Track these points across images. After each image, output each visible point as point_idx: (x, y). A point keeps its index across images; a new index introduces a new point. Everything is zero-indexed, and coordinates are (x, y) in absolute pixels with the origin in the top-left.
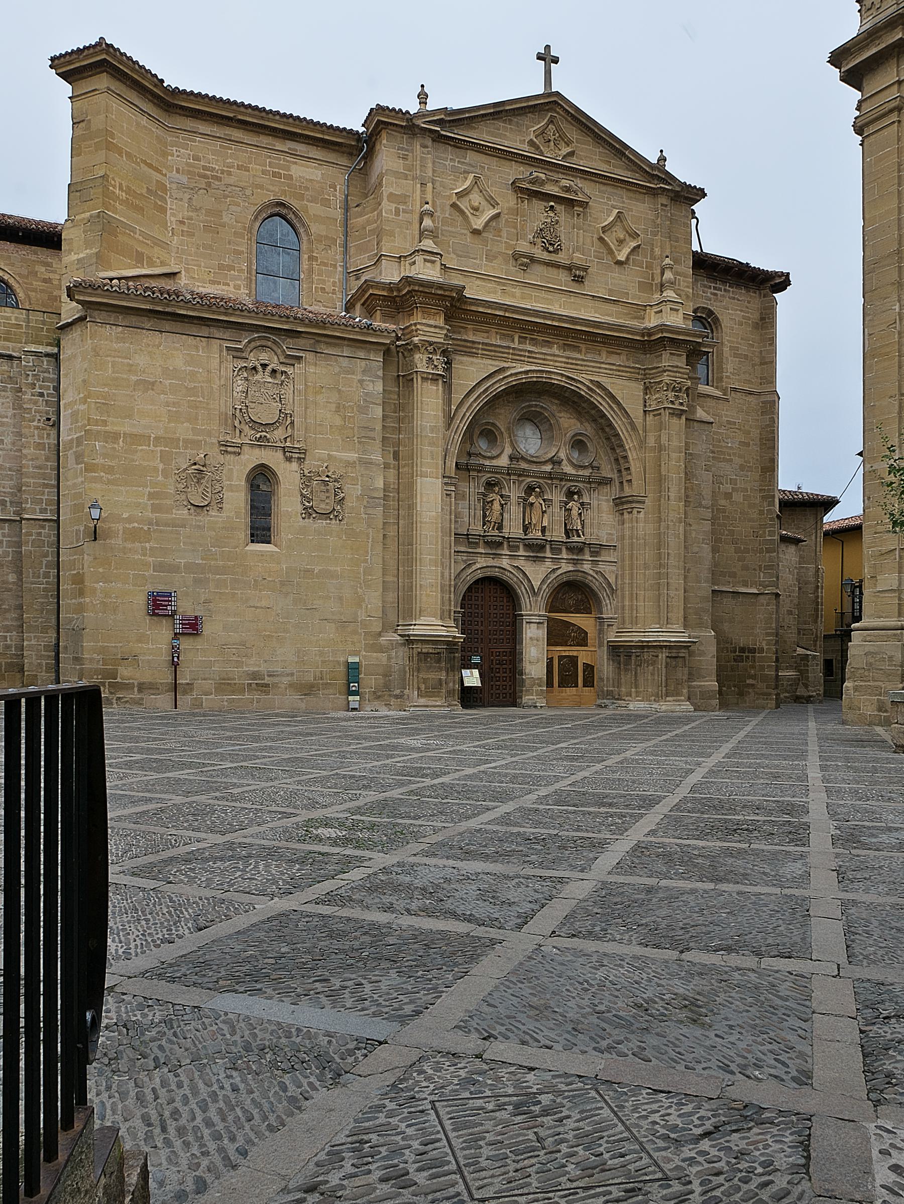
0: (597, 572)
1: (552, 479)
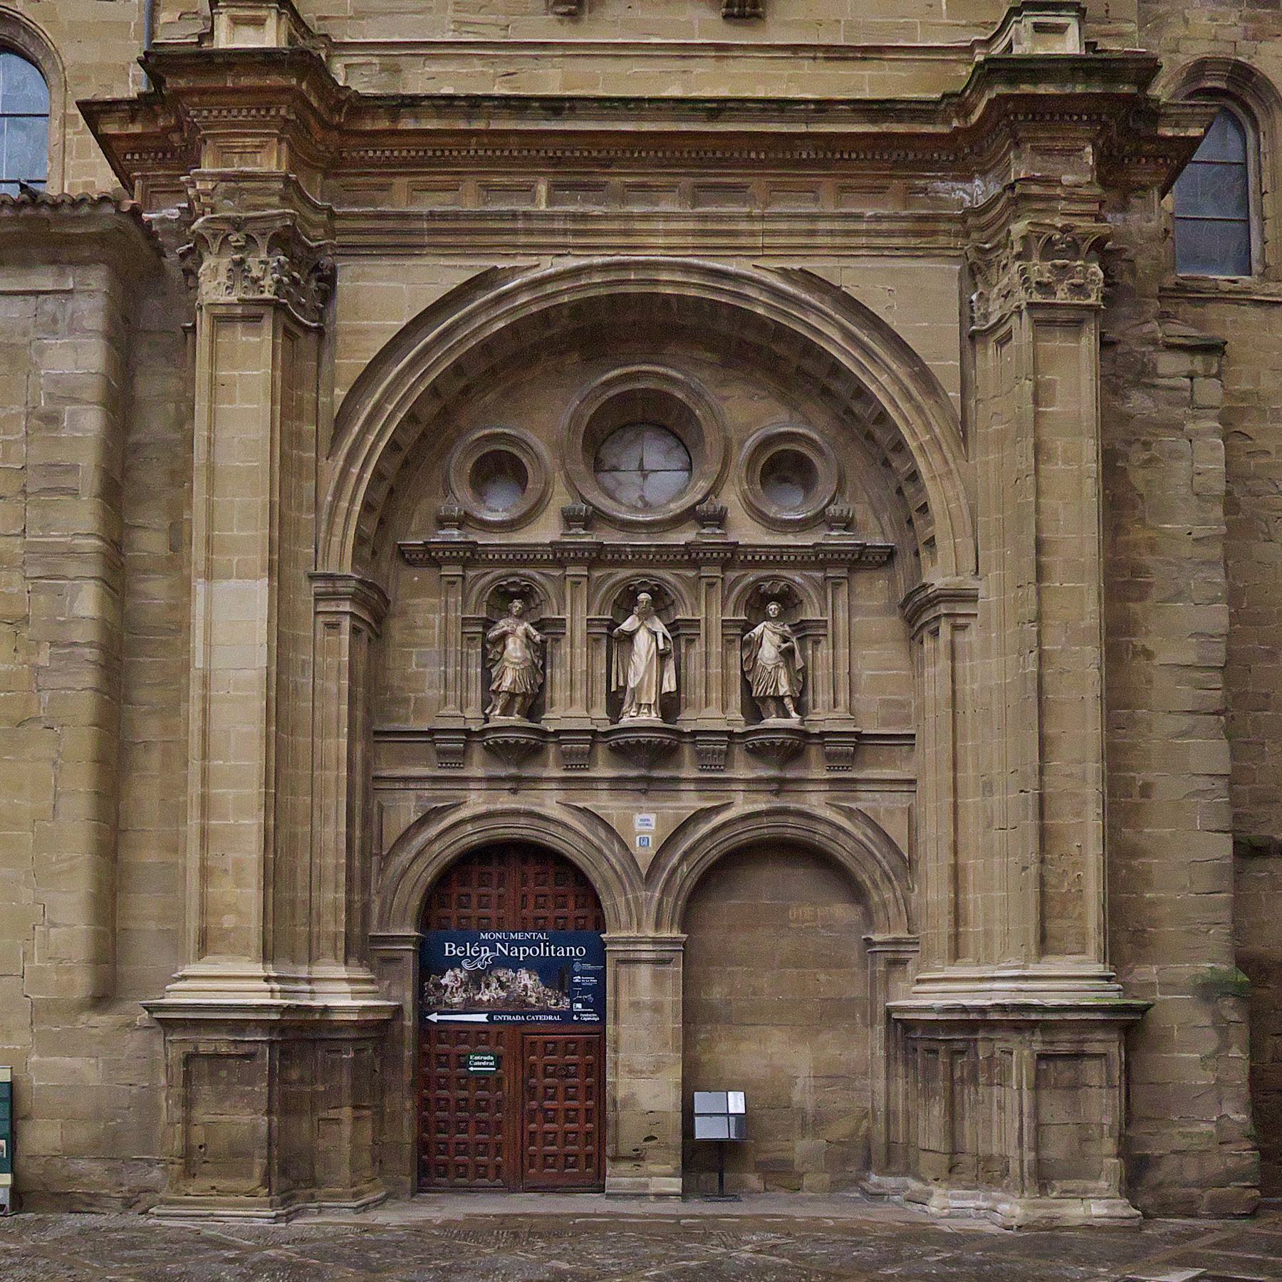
0: (850, 813)
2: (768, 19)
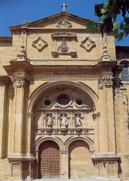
0: (87, 137)
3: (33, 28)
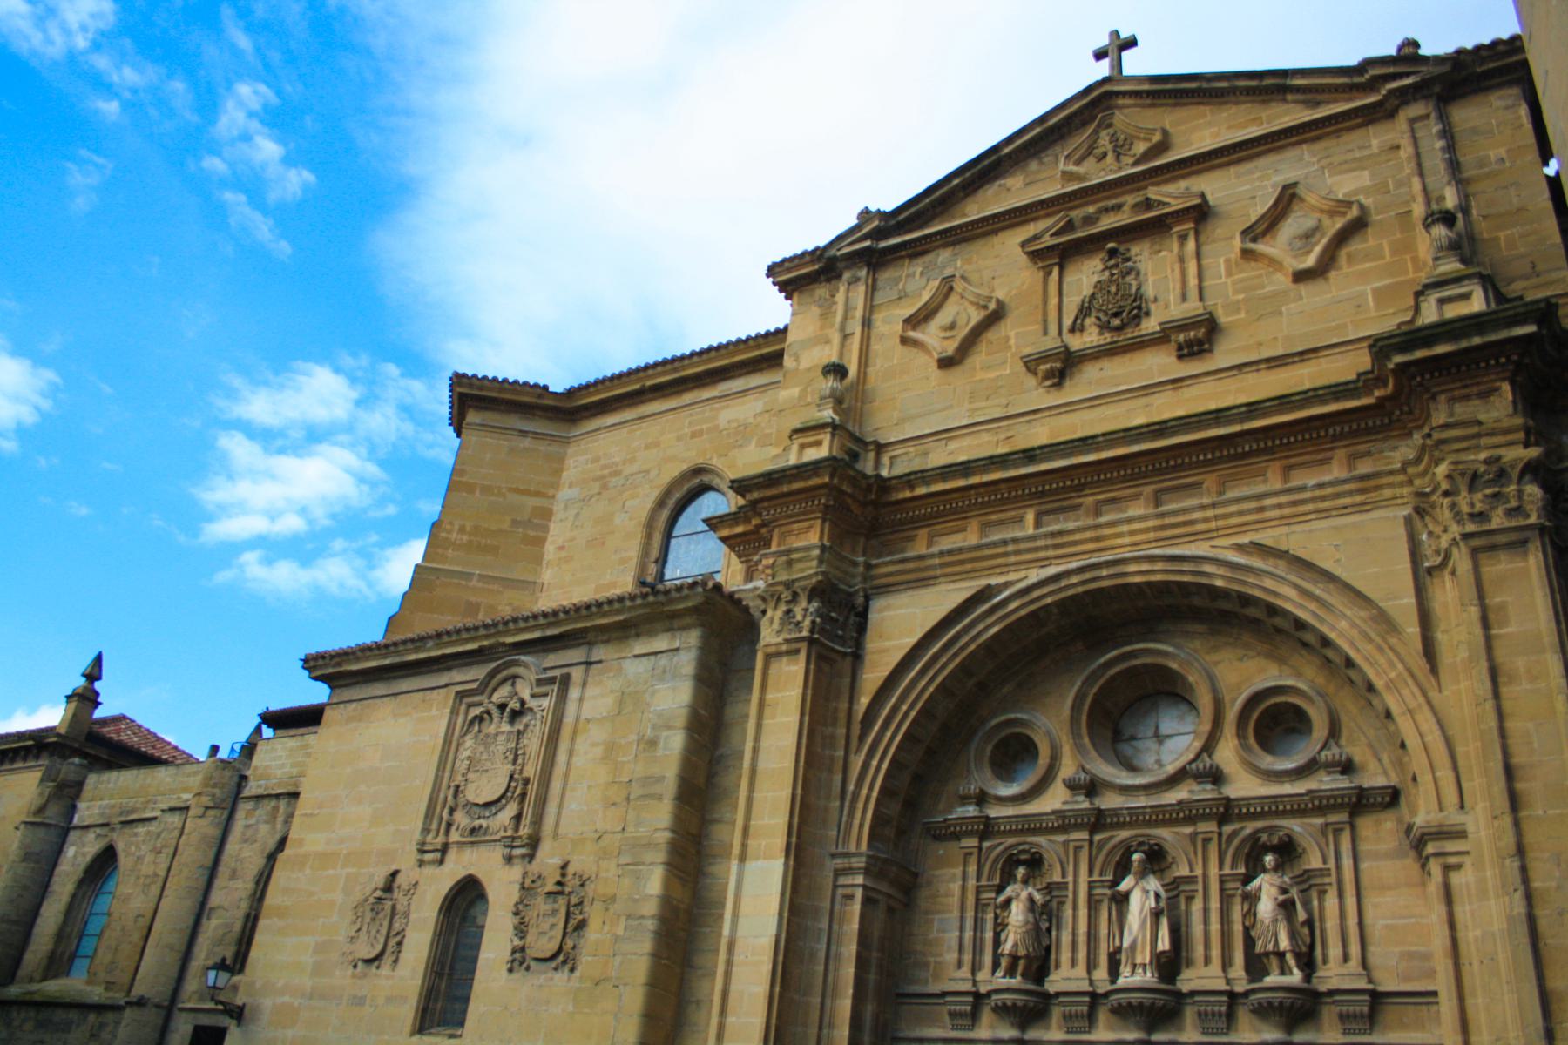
1: (1191, 820)
2: (1215, 352)
3: (907, 237)
